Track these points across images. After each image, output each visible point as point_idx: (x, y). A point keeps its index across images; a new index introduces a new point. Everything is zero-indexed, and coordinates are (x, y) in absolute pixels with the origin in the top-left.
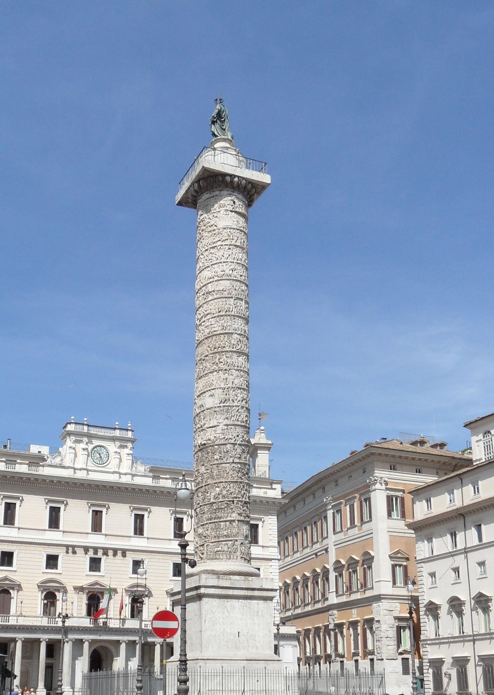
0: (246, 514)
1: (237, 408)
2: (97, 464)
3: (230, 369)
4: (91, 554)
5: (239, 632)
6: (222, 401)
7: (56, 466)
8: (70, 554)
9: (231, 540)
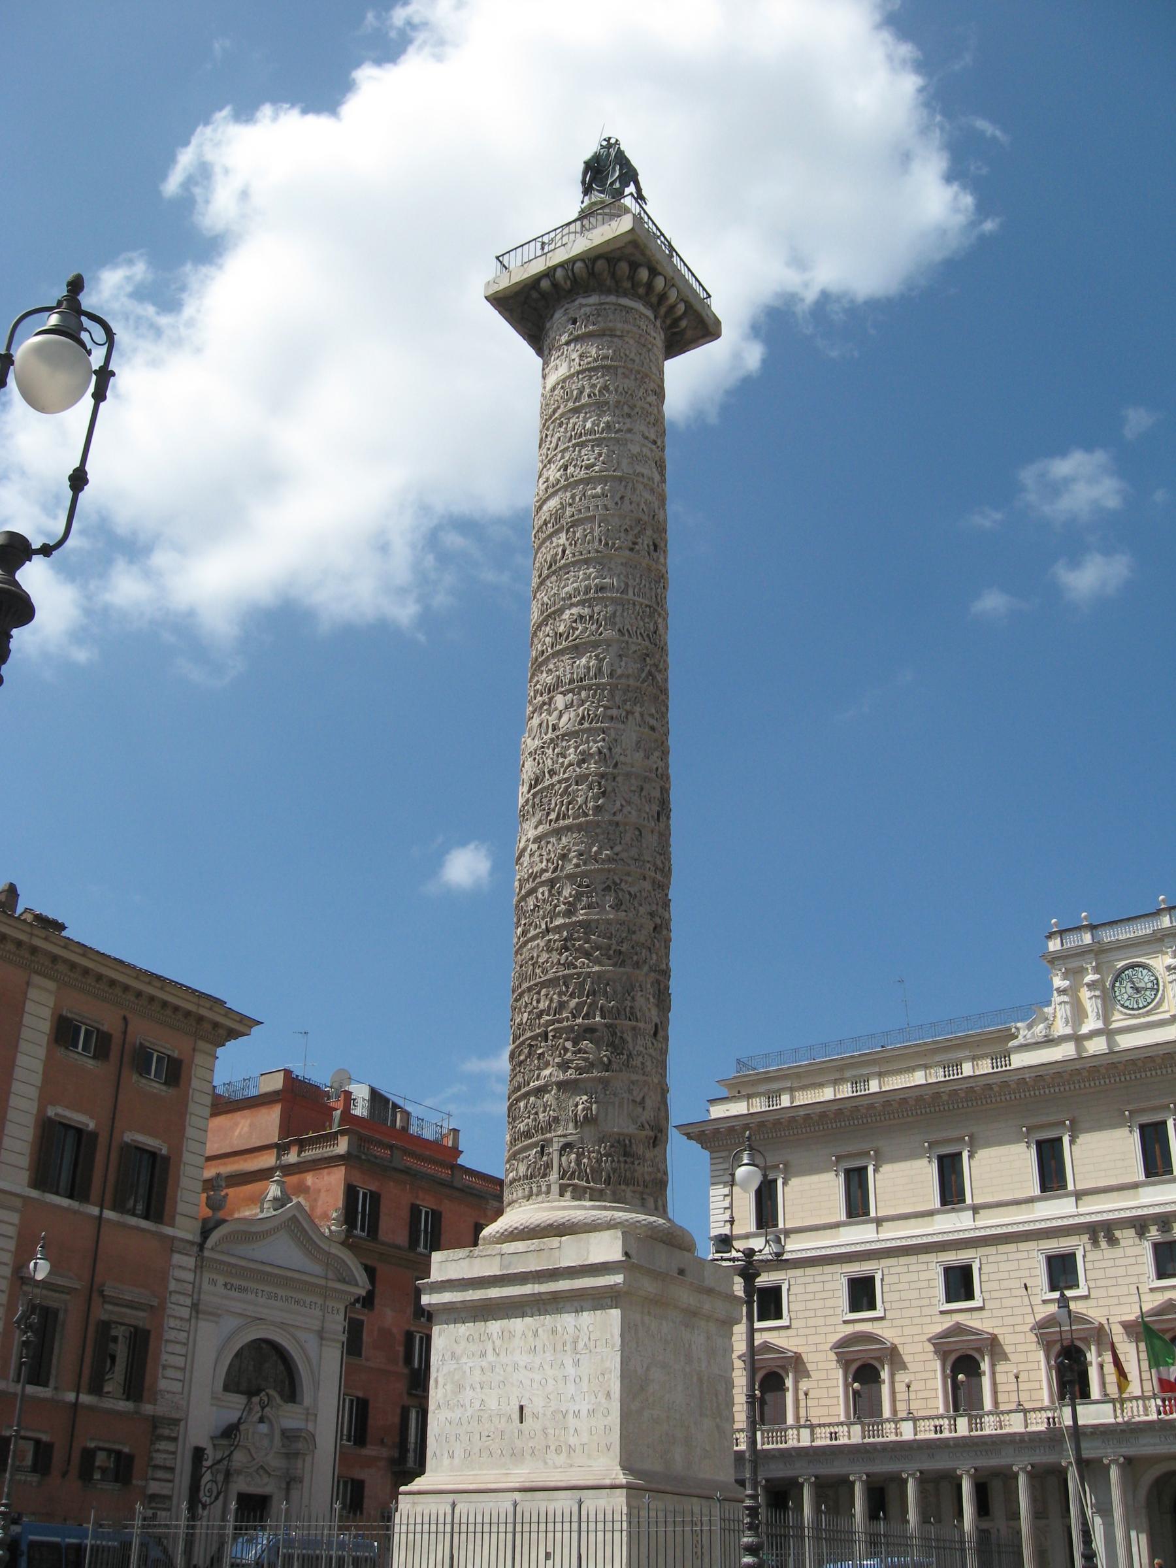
0: (586, 1060)
1: (563, 785)
2: (1133, 1009)
3: (551, 699)
4: (1154, 1232)
5: (521, 1408)
6: (531, 784)
7: (1037, 1045)
8: (1103, 1244)
9: (534, 1145)
